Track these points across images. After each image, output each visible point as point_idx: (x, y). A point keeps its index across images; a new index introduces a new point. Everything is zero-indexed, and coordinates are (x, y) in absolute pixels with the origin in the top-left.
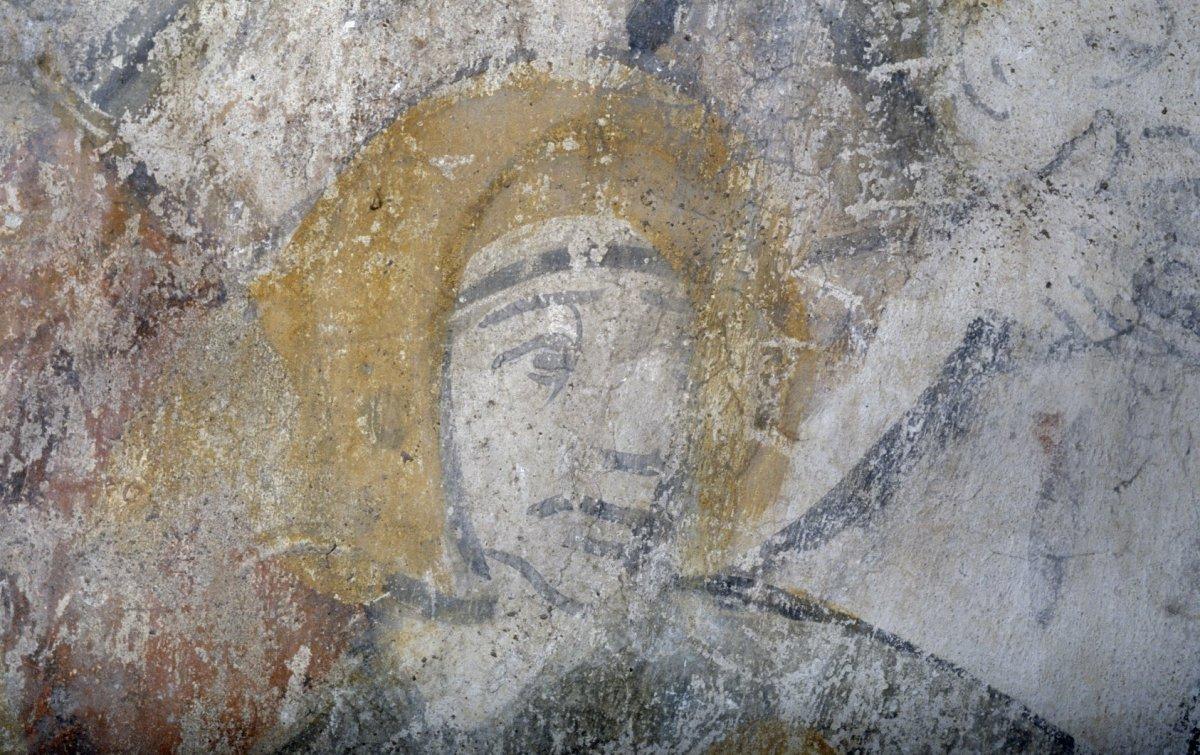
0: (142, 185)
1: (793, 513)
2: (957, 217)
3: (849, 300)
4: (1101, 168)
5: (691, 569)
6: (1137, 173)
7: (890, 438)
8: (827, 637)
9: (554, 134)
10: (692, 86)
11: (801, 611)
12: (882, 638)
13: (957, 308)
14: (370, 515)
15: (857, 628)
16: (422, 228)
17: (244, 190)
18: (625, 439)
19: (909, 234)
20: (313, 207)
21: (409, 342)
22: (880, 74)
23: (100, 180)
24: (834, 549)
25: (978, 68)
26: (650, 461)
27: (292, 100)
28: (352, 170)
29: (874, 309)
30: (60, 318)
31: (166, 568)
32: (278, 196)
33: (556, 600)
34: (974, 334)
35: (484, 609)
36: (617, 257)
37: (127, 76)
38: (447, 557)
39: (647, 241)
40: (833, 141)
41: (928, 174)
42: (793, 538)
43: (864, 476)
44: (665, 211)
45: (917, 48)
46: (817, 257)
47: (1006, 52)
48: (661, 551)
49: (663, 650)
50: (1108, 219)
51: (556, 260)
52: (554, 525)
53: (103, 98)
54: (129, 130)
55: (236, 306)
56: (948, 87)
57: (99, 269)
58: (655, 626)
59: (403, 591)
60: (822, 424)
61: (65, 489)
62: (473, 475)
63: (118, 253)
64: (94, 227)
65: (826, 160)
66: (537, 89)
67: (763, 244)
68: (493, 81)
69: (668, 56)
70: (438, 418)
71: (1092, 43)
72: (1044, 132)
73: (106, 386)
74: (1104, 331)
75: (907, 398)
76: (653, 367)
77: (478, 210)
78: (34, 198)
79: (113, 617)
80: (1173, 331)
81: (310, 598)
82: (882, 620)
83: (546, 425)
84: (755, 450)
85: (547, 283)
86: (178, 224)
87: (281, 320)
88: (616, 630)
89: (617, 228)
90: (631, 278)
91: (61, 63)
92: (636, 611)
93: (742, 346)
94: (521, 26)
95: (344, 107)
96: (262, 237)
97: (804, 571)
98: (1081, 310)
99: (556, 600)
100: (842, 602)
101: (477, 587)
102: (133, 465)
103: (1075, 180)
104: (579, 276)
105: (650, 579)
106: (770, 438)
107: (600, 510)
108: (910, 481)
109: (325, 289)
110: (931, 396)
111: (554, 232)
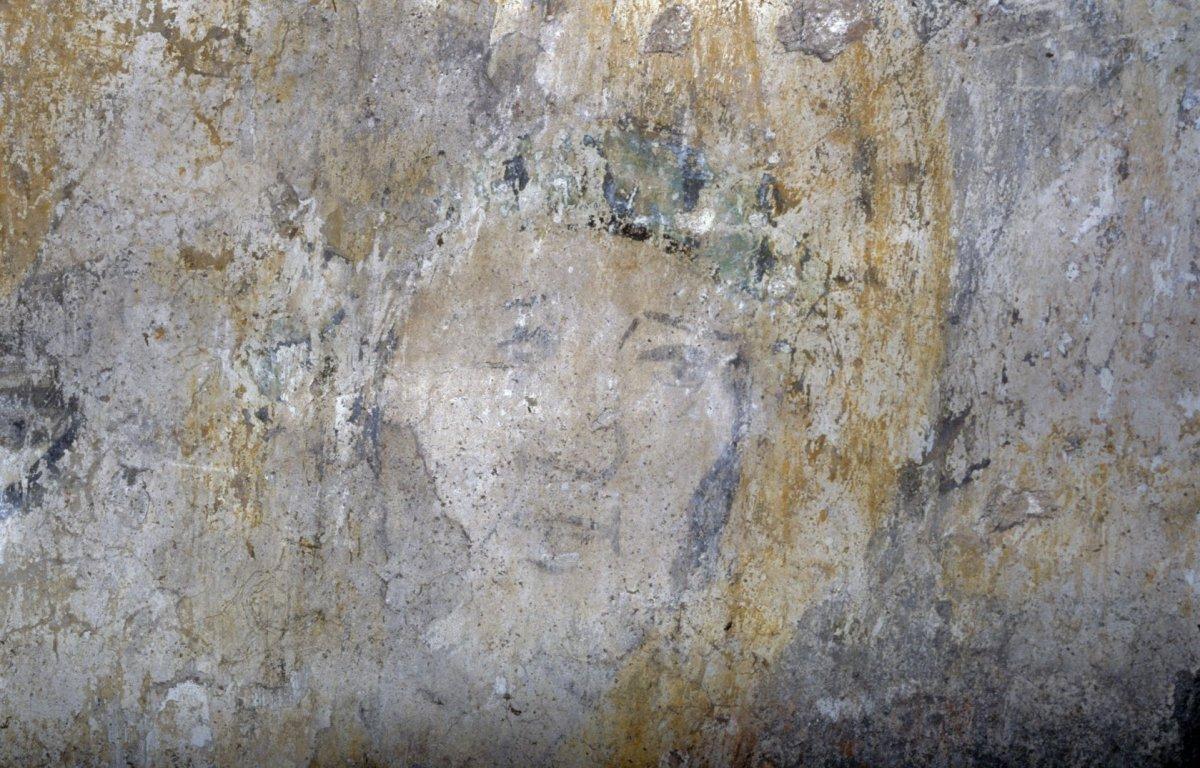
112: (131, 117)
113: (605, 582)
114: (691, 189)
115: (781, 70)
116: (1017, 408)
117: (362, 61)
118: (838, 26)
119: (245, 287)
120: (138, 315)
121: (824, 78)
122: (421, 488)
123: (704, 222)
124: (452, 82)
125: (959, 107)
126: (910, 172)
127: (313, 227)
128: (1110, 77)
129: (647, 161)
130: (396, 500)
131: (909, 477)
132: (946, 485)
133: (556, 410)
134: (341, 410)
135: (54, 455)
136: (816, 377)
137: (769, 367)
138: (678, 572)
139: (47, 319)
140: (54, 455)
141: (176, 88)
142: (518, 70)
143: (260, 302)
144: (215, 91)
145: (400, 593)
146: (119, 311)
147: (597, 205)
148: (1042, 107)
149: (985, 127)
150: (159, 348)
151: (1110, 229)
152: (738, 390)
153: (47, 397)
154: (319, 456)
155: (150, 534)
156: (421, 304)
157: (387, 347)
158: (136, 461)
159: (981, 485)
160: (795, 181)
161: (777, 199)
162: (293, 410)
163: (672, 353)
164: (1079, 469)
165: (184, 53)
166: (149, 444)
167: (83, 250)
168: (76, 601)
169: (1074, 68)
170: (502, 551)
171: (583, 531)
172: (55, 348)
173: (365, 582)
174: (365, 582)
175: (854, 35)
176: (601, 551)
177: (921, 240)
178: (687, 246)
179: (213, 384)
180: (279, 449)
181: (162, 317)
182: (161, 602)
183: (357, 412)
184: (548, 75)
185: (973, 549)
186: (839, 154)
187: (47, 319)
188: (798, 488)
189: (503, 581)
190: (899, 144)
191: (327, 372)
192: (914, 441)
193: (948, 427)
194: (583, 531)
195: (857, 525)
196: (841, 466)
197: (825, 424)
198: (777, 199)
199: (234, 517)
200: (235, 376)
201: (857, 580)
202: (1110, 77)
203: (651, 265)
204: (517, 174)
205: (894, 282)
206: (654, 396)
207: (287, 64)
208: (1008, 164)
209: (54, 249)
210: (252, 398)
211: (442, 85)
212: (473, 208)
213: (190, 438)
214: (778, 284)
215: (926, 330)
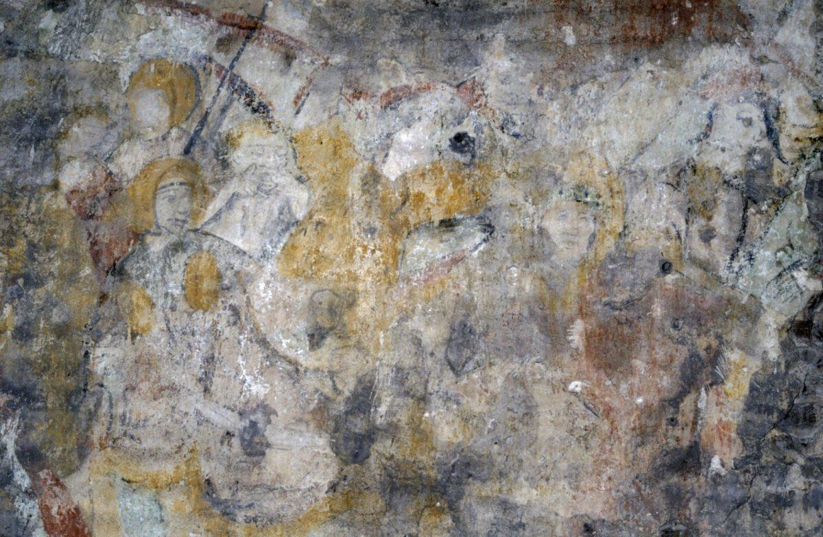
0: (111, 173)
1: (206, 220)
2: (232, 178)
3: (215, 189)
4: (253, 171)
5: (190, 228)
6: (258, 172)
7: (221, 209)
8: (210, 238)
9: (172, 166)
10: (193, 159)
11: (207, 234)
12: (219, 238)
13: (231, 191)
14: (143, 221)
15: (214, 236)
16: (153, 179)
17: (126, 174)
18: (181, 210)
19: (225, 180)
20: (136, 176)
21: (150, 196)
22: (221, 158)
23: (104, 173)
24: (212, 225)
25: (236, 157)
26: (185, 213)
27: (133, 161)
28: (142, 171)
29: (219, 191)
30: (97, 193)
31: (112, 228)
32: (131, 175)
33: (170, 232)
34: (233, 195)
35: (159, 234)
36: (181, 184)
37: (109, 158)
38: (154, 227)
39: (186, 181)
40: (213, 168)
41: (227, 172)
42: (206, 223)
43: (217, 215)
44: (188, 177)
45: (226, 154)
46: (210, 184)
47: (240, 154)
48: (186, 226)
49: (186, 240)
50: (253, 178)
51: (172, 184)
52: (171, 222)
53: (105, 161)
54: (109, 165)
55: (124, 191)
56: (231, 159)
57: (104, 185)
58: (185, 236)
59: (148, 232)
60: (210, 208)
61: (97, 218)
62: (159, 215)
63: (107, 183)
64: (103, 179)
65: (213, 170)
66: (170, 160)
67: (203, 182)
68: (164, 158)
69: (190, 155)
70: (154, 206)
71: (252, 153)
72: (245, 166)
73: (104, 203)
74: (252, 194)
75: (224, 204)
76: (186, 199)
77: (161, 177)
78: (94, 175)
79: (104, 236)
80: (263, 194)
81: (134, 233)
82: (218, 235)
83: (170, 207)
84: (200, 211)
85: (171, 188)
86: (116, 179)
87: (131, 193)
88: (179, 237)
89: (182, 180)
90: (183, 187)
91: (99, 156)
92: (182, 234)
93: (199, 196)
94: (168, 151)
95: (141, 163)
96: (128, 181)
97: (208, 229)
98: (249, 191)
99: (170, 232)
100: (213, 233)
101: (159, 231)
102: (108, 214)
103: (249, 173)
104: (175, 187)
105: (184, 230)
106: (203, 209)
107: (177, 220)
108: (223, 215)
109: (138, 188)
110: (227, 204)
111: (172, 180)
112: (501, 184)
113: (577, 250)
114: (586, 195)
115: (599, 179)
116: (634, 225)
117: (537, 177)
118: (606, 172)
119: (520, 209)
120: (503, 213)
121: (605, 180)
122: (548, 238)
123: (589, 199)
124: (551, 180)
125: (624, 184)
126: (618, 192)
127: (530, 200)
128: (645, 180)
129: (580, 191)
130: (545, 239)
131: (620, 234)
132: (625, 235)
133: (568, 226)
134: (535, 227)
135: (491, 234)
136: (606, 221)
137: (599, 220)
138: (587, 248)
139: (489, 214)
140: (491, 234)
141: (508, 181)
142: (560, 178)
143: (522, 211)
144: (514, 181)
145: (546, 253)
146: (500, 213)
147: (573, 197)
148: (636, 184)
149: (628, 186)
150: (508, 218)
151: (646, 200)
152: (595, 223)
153: (489, 226)
154: (532, 234)
155: (507, 245)
156: (547, 211)
157: (542, 218)
158: (504, 234)
159: (630, 235)
160: (601, 194)
161: (599, 196)
162: (528, 227)
163: (585, 218)
164: (643, 232)
165: (509, 175)
166: (506, 232)
167: (494, 204)
168: (495, 256)
169: (640, 178)
170: (561, 246)
171: (573, 243)
172: (490, 218)
173: (540, 251)
174: (540, 251)
175: (609, 174)
176: (576, 245)
177: (620, 202)
178: (586, 203)
179: (516, 222)
180: (526, 233)
181: (507, 213)
182: (509, 255)
183: (538, 227)
184: (565, 179)
185: (629, 244)
186: (608, 190)
187: (489, 214)
188: (604, 237)
189: (562, 251)
190: (616, 188)
191: (533, 221)
192: (620, 229)
193: (625, 227)
194: (573, 243)
195: (613, 241)
196: (610, 233)
197: (608, 227)
198: (599, 196)
199: (520, 243)
200: (519, 222)
201: (613, 249)
202: (645, 180)
203: (581, 206)
204: (561, 193)
205: (616, 207)
206: (582, 224)
207: (525, 177)
208: (631, 192)
209: (489, 204)
210: (522, 225)
211: (549, 180)
212: (555, 198)
213: (512, 231)
214: (600, 207)
215: (621, 215)
